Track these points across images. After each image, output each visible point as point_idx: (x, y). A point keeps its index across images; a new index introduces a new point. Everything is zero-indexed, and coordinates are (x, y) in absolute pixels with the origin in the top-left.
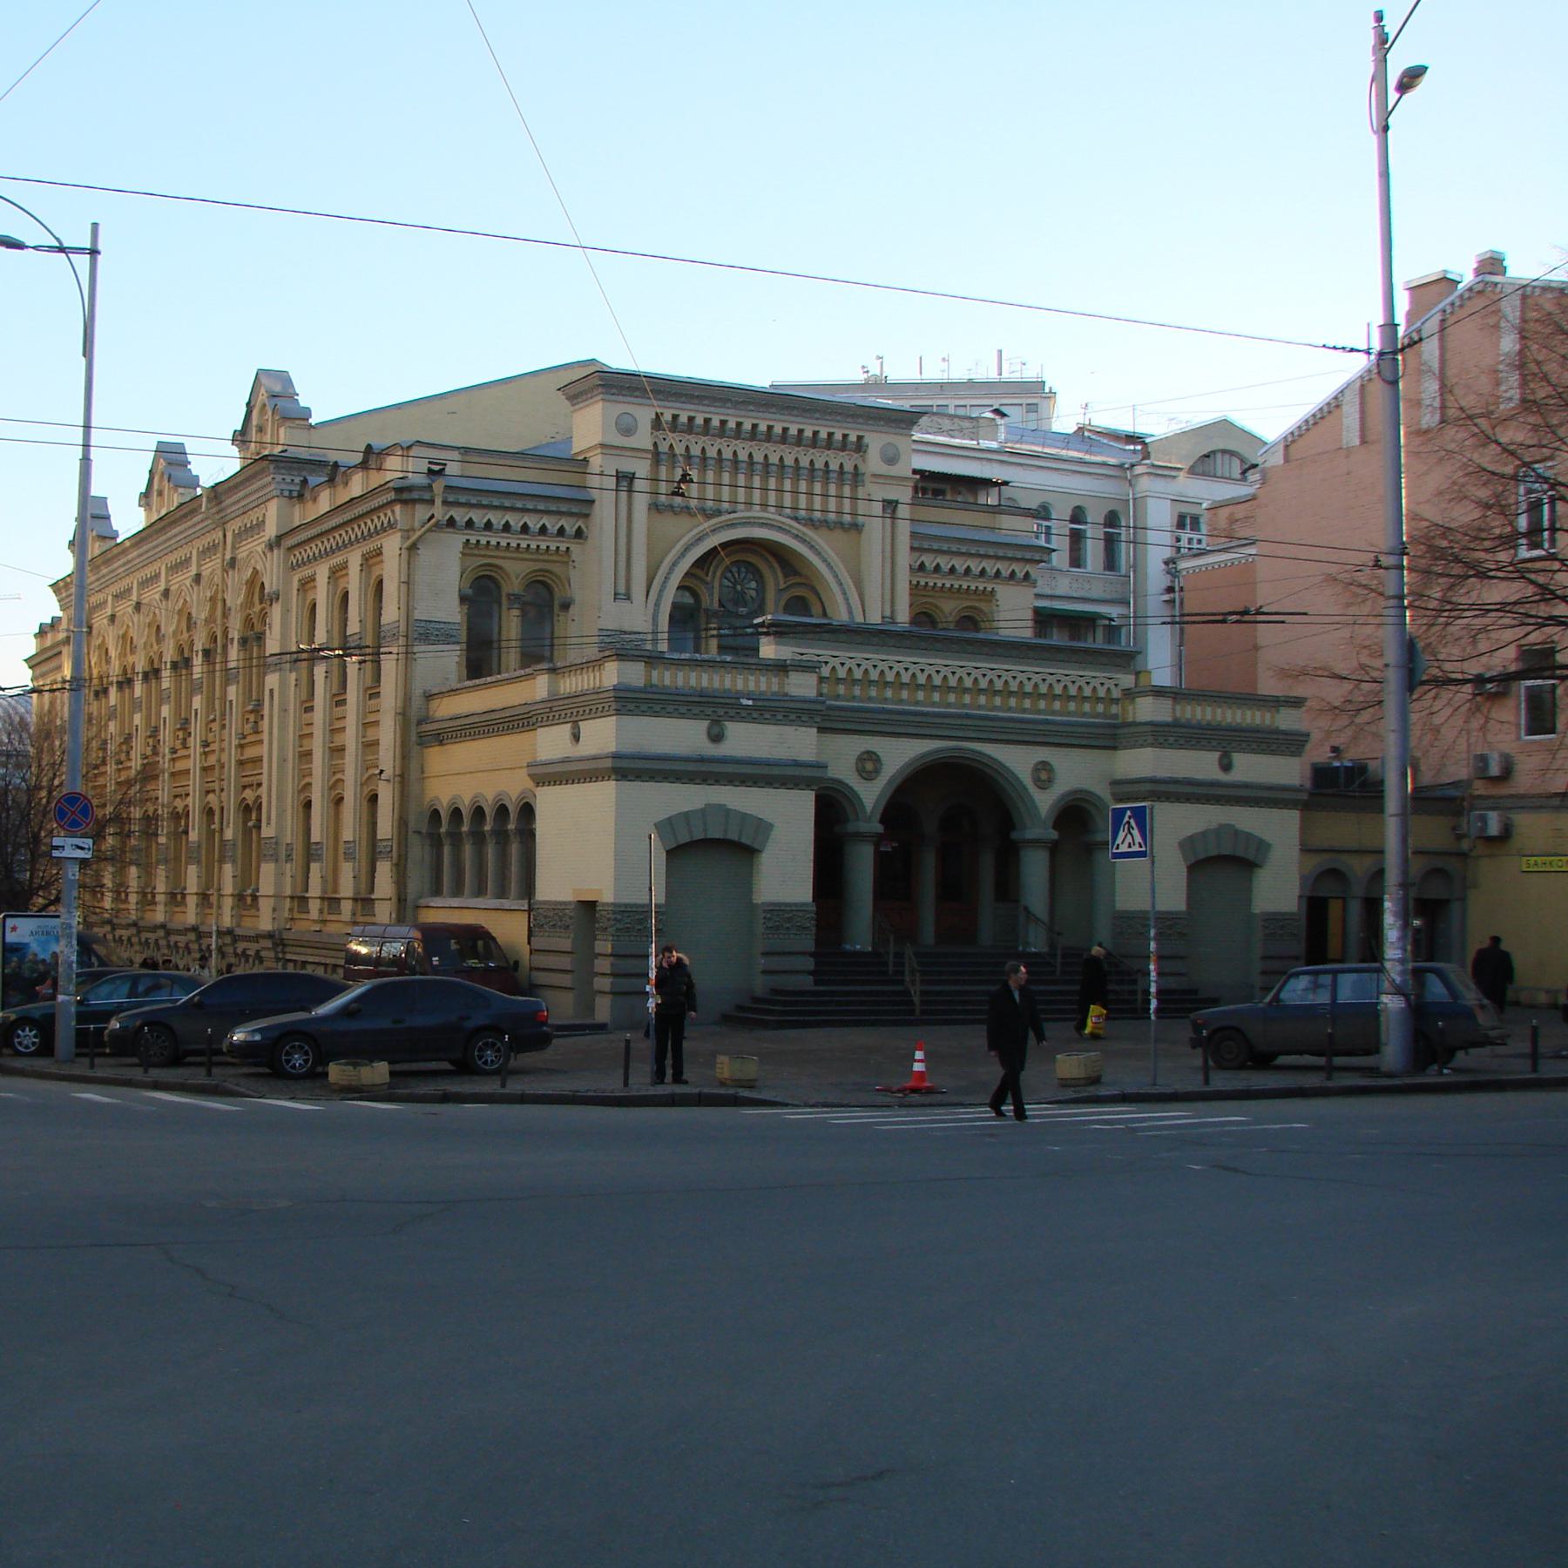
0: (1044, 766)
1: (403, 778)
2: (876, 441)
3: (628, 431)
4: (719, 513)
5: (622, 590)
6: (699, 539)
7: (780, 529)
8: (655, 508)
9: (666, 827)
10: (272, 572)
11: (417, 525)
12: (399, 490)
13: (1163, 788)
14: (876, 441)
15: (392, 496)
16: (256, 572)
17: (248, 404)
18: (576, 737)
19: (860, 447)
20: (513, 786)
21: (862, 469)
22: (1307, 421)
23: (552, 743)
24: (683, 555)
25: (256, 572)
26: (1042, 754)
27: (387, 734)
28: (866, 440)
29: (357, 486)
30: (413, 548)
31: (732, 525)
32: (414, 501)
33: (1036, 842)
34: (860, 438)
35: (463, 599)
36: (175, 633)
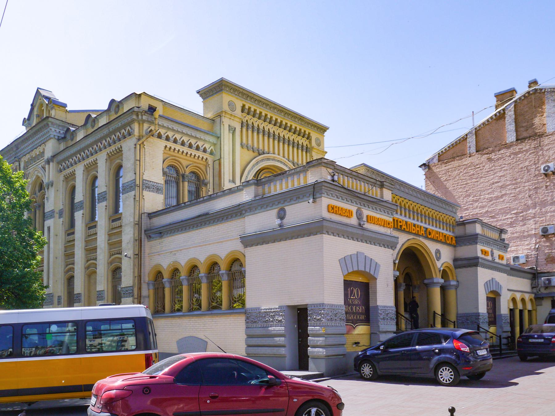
0: (438, 252)
1: (139, 255)
2: (314, 135)
4: (264, 153)
5: (231, 179)
6: (257, 163)
7: (284, 164)
8: (242, 145)
9: (344, 261)
10: (51, 174)
14: (314, 135)
16: (38, 177)
19: (309, 138)
21: (309, 146)
23: (265, 220)
24: (252, 168)
25: (38, 177)
26: (439, 246)
27: (128, 235)
28: (311, 135)
31: (268, 159)
33: (438, 283)
34: (309, 133)
35: (164, 173)
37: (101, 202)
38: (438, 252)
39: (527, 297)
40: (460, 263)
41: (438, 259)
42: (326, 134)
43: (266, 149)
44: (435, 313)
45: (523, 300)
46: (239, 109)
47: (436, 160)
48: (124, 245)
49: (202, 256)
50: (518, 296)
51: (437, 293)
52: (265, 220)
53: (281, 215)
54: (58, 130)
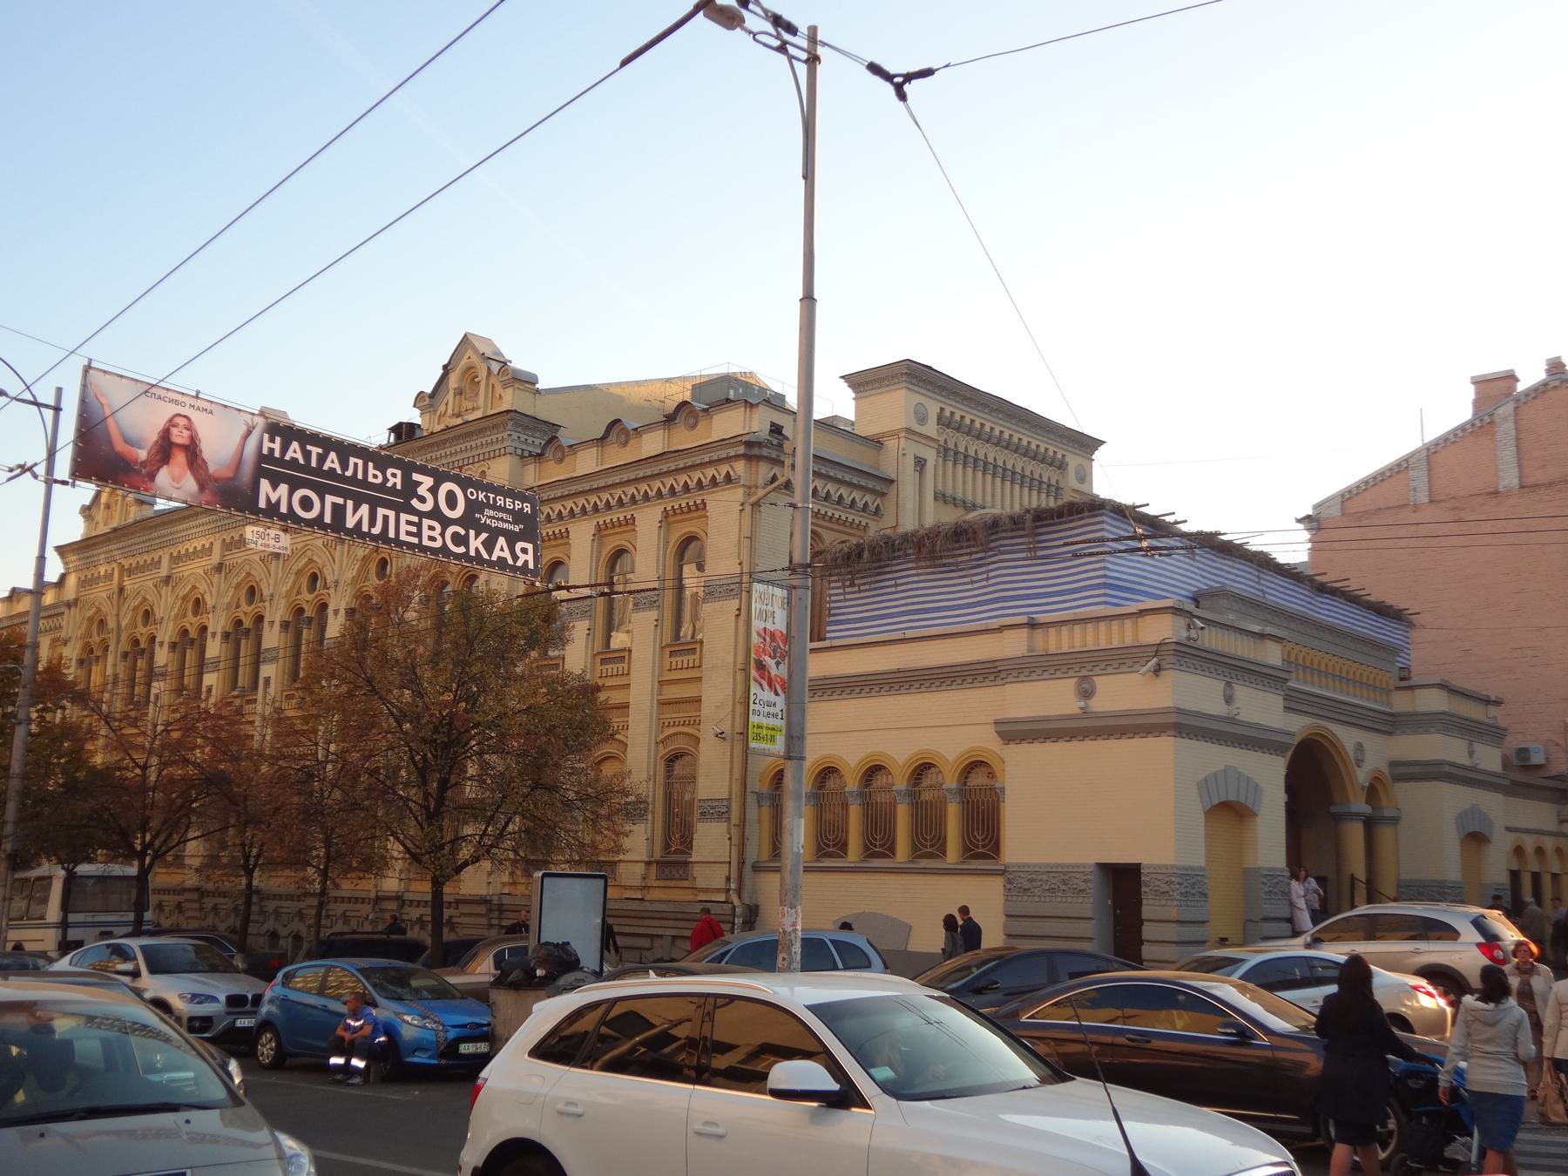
0: (1360, 747)
2: (1073, 461)
3: (922, 420)
11: (760, 482)
12: (749, 444)
13: (1455, 771)
15: (741, 450)
17: (445, 367)
18: (1086, 694)
19: (1061, 466)
20: (951, 748)
21: (1061, 485)
22: (1383, 473)
23: (1053, 698)
29: (653, 444)
30: (756, 505)
32: (760, 458)
36: (289, 593)
37: (644, 610)
38: (1360, 747)
39: (1549, 844)
40: (1402, 770)
41: (1359, 762)
42: (1099, 455)
43: (979, 501)
44: (1353, 879)
45: (1539, 851)
46: (933, 418)
47: (1335, 511)
48: (707, 708)
49: (900, 752)
50: (1529, 843)
51: (1355, 834)
52: (1053, 698)
53: (1086, 694)
54: (523, 437)
